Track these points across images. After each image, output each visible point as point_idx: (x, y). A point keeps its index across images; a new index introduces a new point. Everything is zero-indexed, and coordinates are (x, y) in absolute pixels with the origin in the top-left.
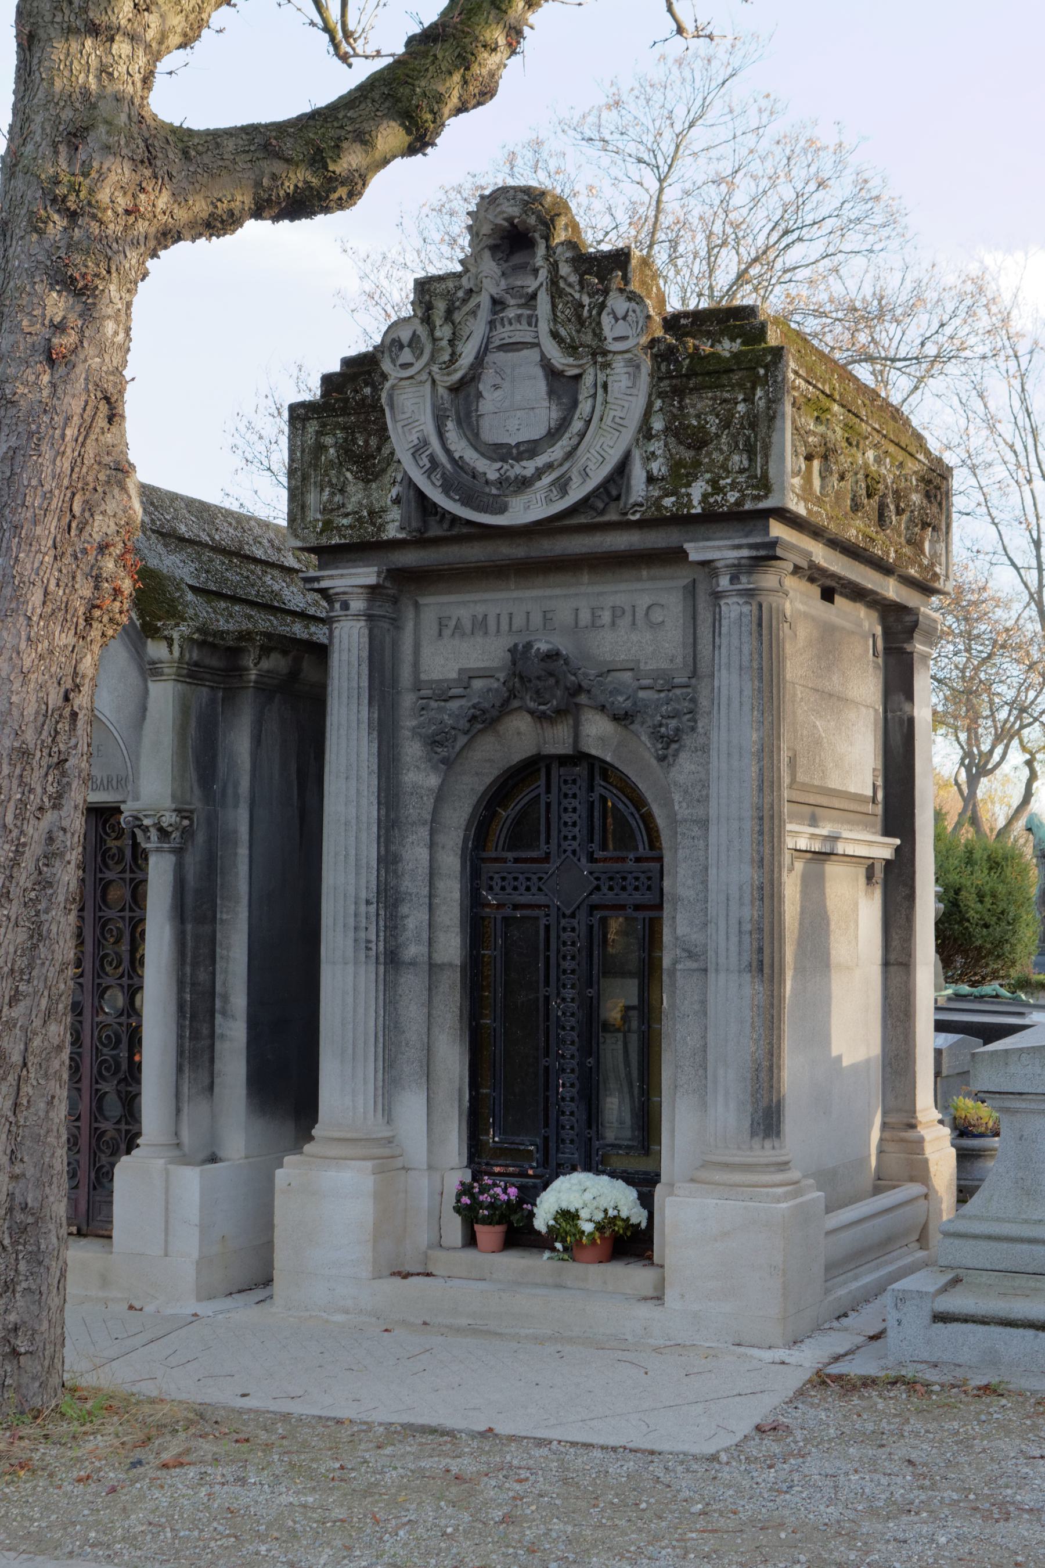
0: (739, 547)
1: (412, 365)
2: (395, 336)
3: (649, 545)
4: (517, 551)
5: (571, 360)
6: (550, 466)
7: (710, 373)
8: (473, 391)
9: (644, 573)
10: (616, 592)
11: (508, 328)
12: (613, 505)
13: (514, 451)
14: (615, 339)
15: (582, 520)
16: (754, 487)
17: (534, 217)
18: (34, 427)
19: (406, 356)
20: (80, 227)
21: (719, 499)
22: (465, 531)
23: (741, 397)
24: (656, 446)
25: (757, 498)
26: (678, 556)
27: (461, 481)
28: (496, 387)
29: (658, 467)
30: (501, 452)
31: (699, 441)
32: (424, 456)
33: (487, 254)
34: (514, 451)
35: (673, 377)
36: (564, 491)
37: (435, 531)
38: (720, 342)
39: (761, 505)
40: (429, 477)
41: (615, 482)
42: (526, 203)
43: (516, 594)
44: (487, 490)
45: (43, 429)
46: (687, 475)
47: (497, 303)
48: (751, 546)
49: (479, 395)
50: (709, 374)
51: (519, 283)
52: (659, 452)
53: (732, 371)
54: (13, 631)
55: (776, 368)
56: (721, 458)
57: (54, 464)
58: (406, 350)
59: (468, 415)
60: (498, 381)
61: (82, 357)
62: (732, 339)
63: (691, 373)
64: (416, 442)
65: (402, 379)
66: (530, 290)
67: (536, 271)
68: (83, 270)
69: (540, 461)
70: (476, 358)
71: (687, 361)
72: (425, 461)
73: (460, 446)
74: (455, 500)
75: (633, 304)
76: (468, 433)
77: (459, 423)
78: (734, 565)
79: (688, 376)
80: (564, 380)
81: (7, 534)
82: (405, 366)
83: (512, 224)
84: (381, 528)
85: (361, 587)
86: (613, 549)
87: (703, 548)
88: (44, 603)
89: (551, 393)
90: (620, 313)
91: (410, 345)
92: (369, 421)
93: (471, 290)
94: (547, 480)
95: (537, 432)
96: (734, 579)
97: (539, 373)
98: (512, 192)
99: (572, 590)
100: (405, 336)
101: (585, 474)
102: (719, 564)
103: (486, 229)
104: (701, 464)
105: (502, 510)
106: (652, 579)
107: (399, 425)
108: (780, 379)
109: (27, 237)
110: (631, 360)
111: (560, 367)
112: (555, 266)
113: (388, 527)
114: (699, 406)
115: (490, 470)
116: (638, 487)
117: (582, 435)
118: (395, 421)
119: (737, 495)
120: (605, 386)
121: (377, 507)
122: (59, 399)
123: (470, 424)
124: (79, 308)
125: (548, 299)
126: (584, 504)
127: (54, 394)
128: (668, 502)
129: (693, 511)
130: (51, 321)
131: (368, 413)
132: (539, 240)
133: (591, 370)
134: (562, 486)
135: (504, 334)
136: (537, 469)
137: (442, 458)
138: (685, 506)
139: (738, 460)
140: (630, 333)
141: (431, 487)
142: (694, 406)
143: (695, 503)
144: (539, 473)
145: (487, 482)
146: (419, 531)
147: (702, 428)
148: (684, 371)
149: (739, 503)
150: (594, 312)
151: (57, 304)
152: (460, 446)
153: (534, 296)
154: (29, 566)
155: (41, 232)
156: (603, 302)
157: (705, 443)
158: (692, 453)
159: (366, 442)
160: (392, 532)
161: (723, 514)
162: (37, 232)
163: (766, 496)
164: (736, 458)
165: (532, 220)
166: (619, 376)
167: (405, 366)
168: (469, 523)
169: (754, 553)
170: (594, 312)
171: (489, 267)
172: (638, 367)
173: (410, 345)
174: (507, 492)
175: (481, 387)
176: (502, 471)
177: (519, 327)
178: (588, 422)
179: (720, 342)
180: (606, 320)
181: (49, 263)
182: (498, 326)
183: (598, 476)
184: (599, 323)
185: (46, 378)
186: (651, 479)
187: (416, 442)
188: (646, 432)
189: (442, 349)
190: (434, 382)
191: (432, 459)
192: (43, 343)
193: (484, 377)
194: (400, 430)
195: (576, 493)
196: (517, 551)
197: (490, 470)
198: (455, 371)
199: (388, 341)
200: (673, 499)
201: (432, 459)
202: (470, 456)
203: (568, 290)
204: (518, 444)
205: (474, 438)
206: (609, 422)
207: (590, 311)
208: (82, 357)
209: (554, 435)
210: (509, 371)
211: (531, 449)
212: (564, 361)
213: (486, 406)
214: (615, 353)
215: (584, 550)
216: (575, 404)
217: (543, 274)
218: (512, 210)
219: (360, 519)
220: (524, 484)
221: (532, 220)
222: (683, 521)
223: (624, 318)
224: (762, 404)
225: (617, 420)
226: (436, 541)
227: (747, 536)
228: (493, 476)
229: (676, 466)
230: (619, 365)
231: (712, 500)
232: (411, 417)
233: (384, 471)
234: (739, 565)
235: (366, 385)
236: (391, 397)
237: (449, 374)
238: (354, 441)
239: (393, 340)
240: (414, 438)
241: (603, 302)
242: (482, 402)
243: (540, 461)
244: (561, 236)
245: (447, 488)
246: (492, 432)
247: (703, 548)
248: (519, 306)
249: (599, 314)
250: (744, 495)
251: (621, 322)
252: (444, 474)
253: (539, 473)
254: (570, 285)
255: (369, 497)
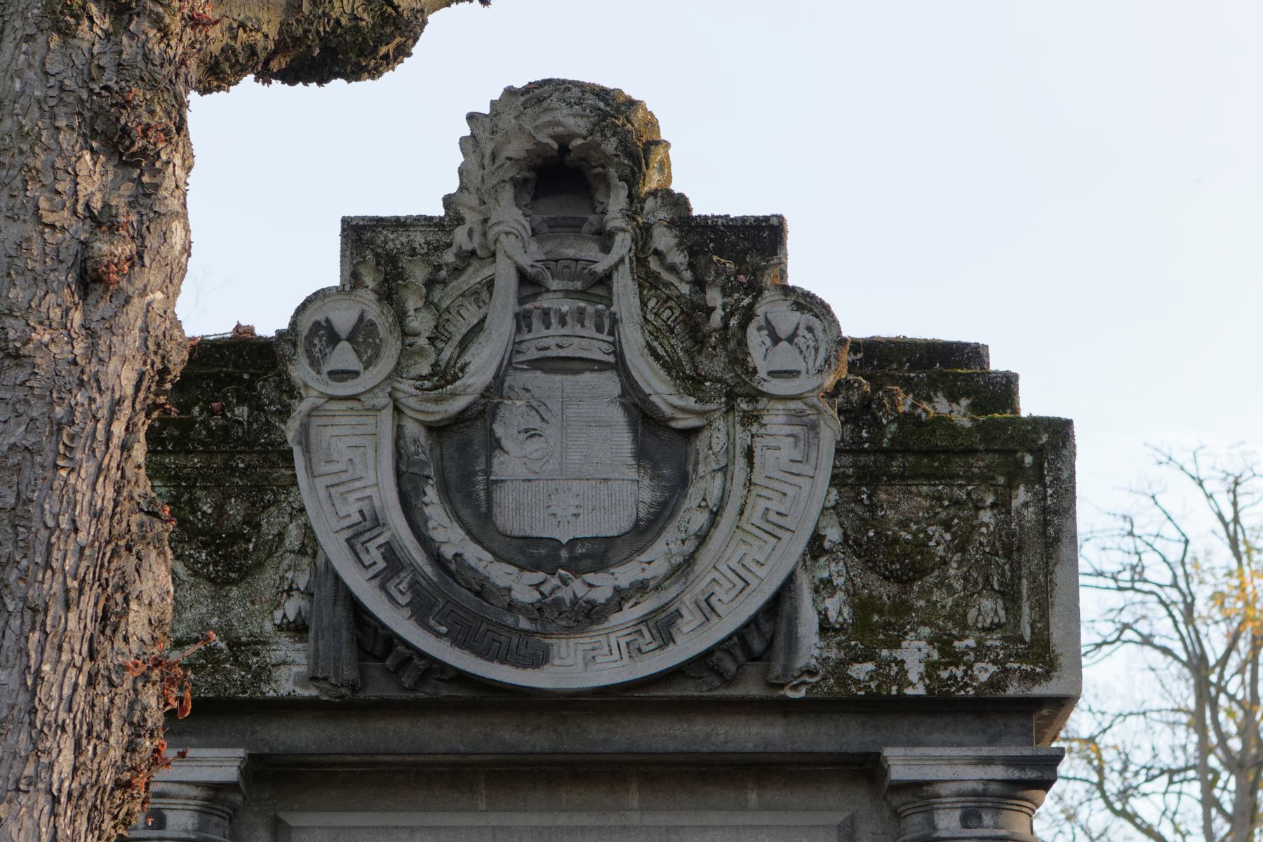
0: (987, 761)
1: (355, 374)
2: (320, 317)
3: (802, 747)
4: (533, 738)
5: (690, 402)
6: (641, 587)
7: (929, 452)
8: (477, 435)
9: (753, 797)
10: (705, 828)
11: (556, 329)
12: (753, 669)
13: (564, 554)
14: (773, 374)
15: (691, 690)
16: (1020, 657)
17: (614, 141)
18: (59, 411)
19: (344, 356)
20: (132, 36)
21: (959, 673)
22: (444, 692)
23: (990, 499)
24: (828, 569)
25: (1032, 678)
26: (865, 769)
27: (452, 597)
28: (531, 433)
29: (835, 606)
30: (534, 553)
31: (908, 566)
32: (372, 546)
33: (508, 194)
34: (564, 554)
35: (867, 452)
36: (665, 635)
37: (381, 688)
38: (930, 400)
39: (1038, 690)
40: (383, 587)
41: (758, 628)
42: (604, 116)
43: (494, 819)
44: (510, 620)
45: (78, 417)
46: (886, 626)
47: (528, 283)
48: (1009, 762)
49: (494, 444)
50: (931, 453)
51: (571, 252)
52: (839, 581)
53: (971, 451)
54: (28, 823)
55: (1058, 457)
56: (949, 602)
57: (94, 489)
58: (344, 346)
59: (467, 477)
60: (535, 422)
61: (139, 284)
62: (953, 398)
63: (900, 447)
64: (356, 518)
65: (332, 398)
66: (600, 268)
67: (605, 239)
68: (145, 119)
69: (626, 575)
70: (496, 377)
71: (893, 427)
72: (374, 555)
73: (451, 537)
74: (439, 635)
75: (807, 318)
76: (465, 513)
77: (445, 491)
78: (975, 793)
79: (890, 453)
80: (665, 436)
81: (15, 623)
82: (340, 375)
83: (564, 149)
84: (262, 673)
85: (197, 784)
86: (730, 747)
87: (922, 758)
88: (75, 769)
89: (641, 455)
90: (784, 329)
91: (351, 338)
92: (234, 470)
93: (473, 253)
94: (631, 613)
95: (614, 523)
96: (970, 818)
97: (618, 416)
98: (576, 92)
99: (614, 820)
100: (344, 319)
101: (708, 608)
102: (944, 790)
103: (516, 148)
104: (911, 608)
105: (539, 659)
106: (770, 807)
107: (321, 483)
108: (1065, 475)
109: (41, 39)
110: (799, 414)
111: (668, 411)
112: (645, 231)
113: (276, 673)
114: (905, 506)
115: (522, 586)
116: (810, 646)
117: (702, 538)
118: (312, 474)
119: (993, 669)
120: (749, 454)
121: (242, 633)
122: (101, 360)
123: (470, 496)
124: (127, 189)
125: (632, 287)
126: (703, 663)
127: (92, 348)
128: (861, 671)
129: (909, 691)
130: (87, 206)
131: (232, 454)
132: (615, 181)
133: (720, 424)
134: (663, 627)
135: (548, 339)
136: (617, 590)
137: (418, 555)
138: (895, 680)
139: (988, 607)
140: (799, 365)
141: (387, 605)
142: (895, 506)
143: (913, 676)
144: (620, 598)
145: (512, 607)
146: (353, 688)
147: (921, 545)
148: (885, 443)
149: (993, 683)
150: (733, 322)
151: (93, 178)
152: (451, 537)
153: (605, 280)
154: (55, 692)
155: (67, 33)
156: (751, 306)
157: (922, 573)
158: (894, 588)
159: (219, 508)
160: (285, 684)
161: (966, 700)
162: (59, 31)
163: (1047, 676)
164: (987, 604)
165: (610, 146)
166: (777, 437)
167: (340, 375)
168: (462, 678)
169: (1015, 774)
170: (733, 322)
171: (509, 215)
172: (813, 427)
173: (351, 338)
174: (551, 628)
175: (499, 430)
176: (546, 589)
177: (578, 330)
178: (715, 516)
179: (930, 400)
180: (756, 338)
181: (85, 96)
182: (536, 323)
183: (735, 613)
184: (742, 343)
185: (77, 317)
186: (825, 628)
187: (356, 518)
188: (816, 547)
189: (421, 352)
190: (397, 410)
191: (391, 552)
192: (75, 247)
193: (503, 412)
194: (323, 494)
195: (692, 641)
196: (533, 738)
197: (522, 586)
198: (453, 395)
199: (305, 327)
200: (870, 666)
201: (391, 552)
202: (475, 554)
203: (666, 276)
204: (573, 542)
205: (480, 523)
206: (756, 518)
207: (726, 320)
208: (139, 284)
209: (646, 530)
210: (556, 408)
211: (598, 553)
212: (675, 401)
213: (508, 465)
214: (773, 397)
215: (672, 747)
216: (682, 482)
217: (622, 245)
218: (574, 122)
219: (210, 652)
220: (590, 615)
221: (610, 146)
222: (887, 707)
223: (790, 339)
224: (1030, 514)
225: (773, 517)
226: (384, 708)
227: (991, 742)
228: (523, 594)
229: (863, 607)
230: (776, 420)
231: (944, 674)
232: (345, 473)
233: (260, 565)
234: (984, 794)
235: (240, 403)
236: (305, 429)
237: (437, 401)
238: (193, 504)
239: (317, 324)
240: (352, 510)
241: (751, 306)
242: (498, 459)
243: (626, 575)
244: (653, 181)
245: (421, 611)
246: (519, 513)
247: (922, 758)
248: (568, 293)
249: (743, 326)
250: (1007, 670)
251: (784, 344)
252: (413, 585)
253: (620, 598)
254: (672, 269)
255: (222, 614)
